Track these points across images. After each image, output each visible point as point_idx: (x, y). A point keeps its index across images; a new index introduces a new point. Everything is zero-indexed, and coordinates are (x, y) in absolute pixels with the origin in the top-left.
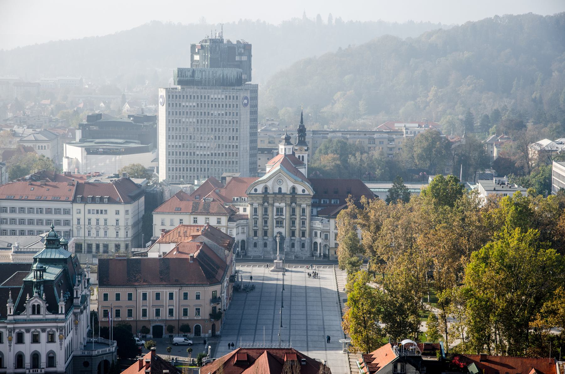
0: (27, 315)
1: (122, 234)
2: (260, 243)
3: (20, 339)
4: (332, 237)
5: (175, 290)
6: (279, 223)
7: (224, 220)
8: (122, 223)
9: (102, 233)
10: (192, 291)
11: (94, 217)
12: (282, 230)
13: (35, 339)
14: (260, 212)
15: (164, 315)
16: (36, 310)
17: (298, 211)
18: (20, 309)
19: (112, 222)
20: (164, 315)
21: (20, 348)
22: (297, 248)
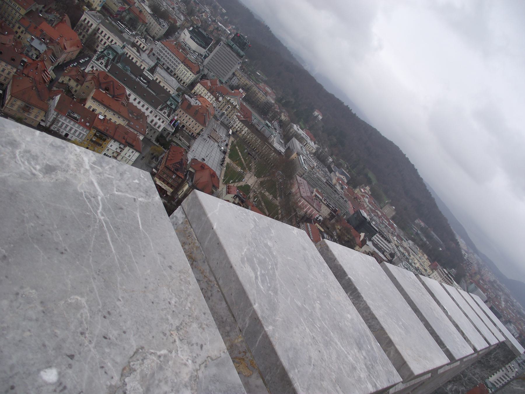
0: (162, 112)
1: (188, 81)
2: (218, 111)
3: (156, 116)
4: (236, 125)
5: (194, 121)
6: (226, 110)
7: (214, 99)
8: (190, 78)
9: (183, 76)
10: (198, 124)
11: (184, 71)
12: (226, 113)
13: (159, 119)
14: (224, 104)
15: (188, 124)
16: (165, 113)
17: (233, 111)
18: (161, 110)
19: (188, 76)
20: (188, 124)
21: (154, 118)
22: (226, 119)
